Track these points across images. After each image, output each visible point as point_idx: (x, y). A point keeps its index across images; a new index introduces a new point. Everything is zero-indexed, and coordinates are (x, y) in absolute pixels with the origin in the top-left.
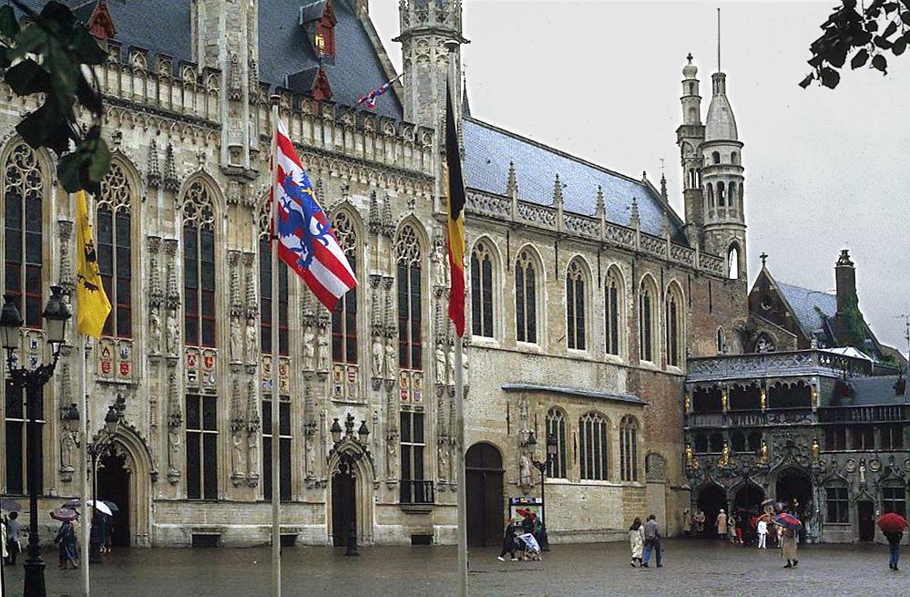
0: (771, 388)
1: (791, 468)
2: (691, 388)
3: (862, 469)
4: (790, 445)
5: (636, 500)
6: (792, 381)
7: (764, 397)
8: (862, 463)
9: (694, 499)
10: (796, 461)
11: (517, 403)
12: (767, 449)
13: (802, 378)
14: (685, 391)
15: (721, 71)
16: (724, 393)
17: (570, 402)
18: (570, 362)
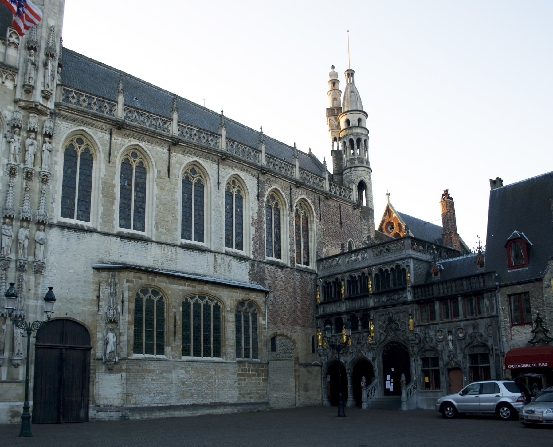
0: (376, 275)
1: (392, 342)
2: (320, 282)
3: (450, 337)
4: (391, 321)
5: (254, 375)
6: (391, 266)
7: (370, 282)
8: (450, 332)
9: (322, 372)
10: (396, 335)
11: (107, 282)
12: (374, 328)
13: (399, 262)
14: (317, 286)
15: (351, 68)
16: (342, 283)
17: (171, 283)
18: (180, 250)
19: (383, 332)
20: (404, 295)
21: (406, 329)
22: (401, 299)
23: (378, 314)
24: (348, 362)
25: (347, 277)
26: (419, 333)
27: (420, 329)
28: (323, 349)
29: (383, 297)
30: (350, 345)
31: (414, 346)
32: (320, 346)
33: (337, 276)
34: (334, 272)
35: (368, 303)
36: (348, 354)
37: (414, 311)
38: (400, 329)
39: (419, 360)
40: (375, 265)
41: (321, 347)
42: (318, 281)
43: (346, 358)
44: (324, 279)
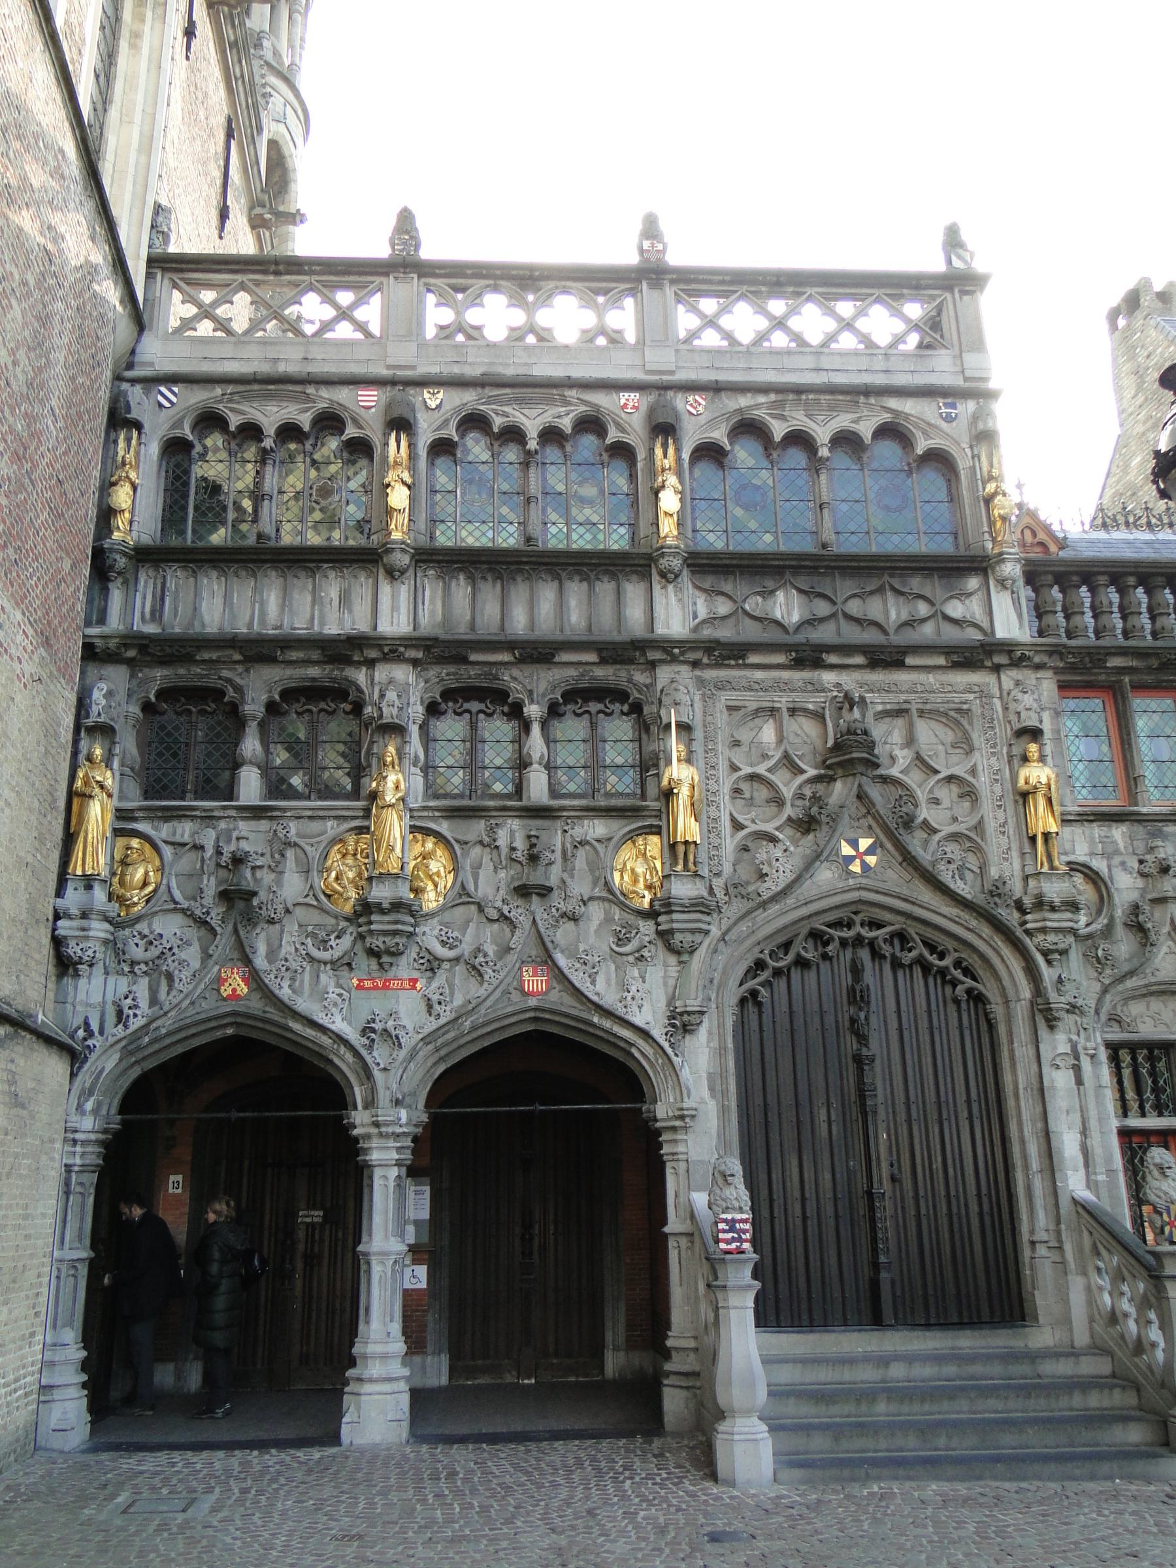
6: (843, 421)
16: (396, 449)
19: (769, 827)
20: (955, 609)
21: (979, 827)
22: (928, 629)
23: (725, 698)
24: (408, 1041)
25: (438, 418)
26: (1099, 865)
27: (1106, 840)
28: (113, 909)
29: (772, 592)
30: (431, 900)
31: (1064, 952)
32: (88, 882)
33: (342, 395)
34: (314, 368)
35: (635, 614)
36: (404, 969)
37: (1046, 716)
38: (925, 822)
39: (1103, 1054)
40: (715, 389)
41: (99, 894)
42: (135, 394)
43: (373, 1005)
44: (199, 397)
